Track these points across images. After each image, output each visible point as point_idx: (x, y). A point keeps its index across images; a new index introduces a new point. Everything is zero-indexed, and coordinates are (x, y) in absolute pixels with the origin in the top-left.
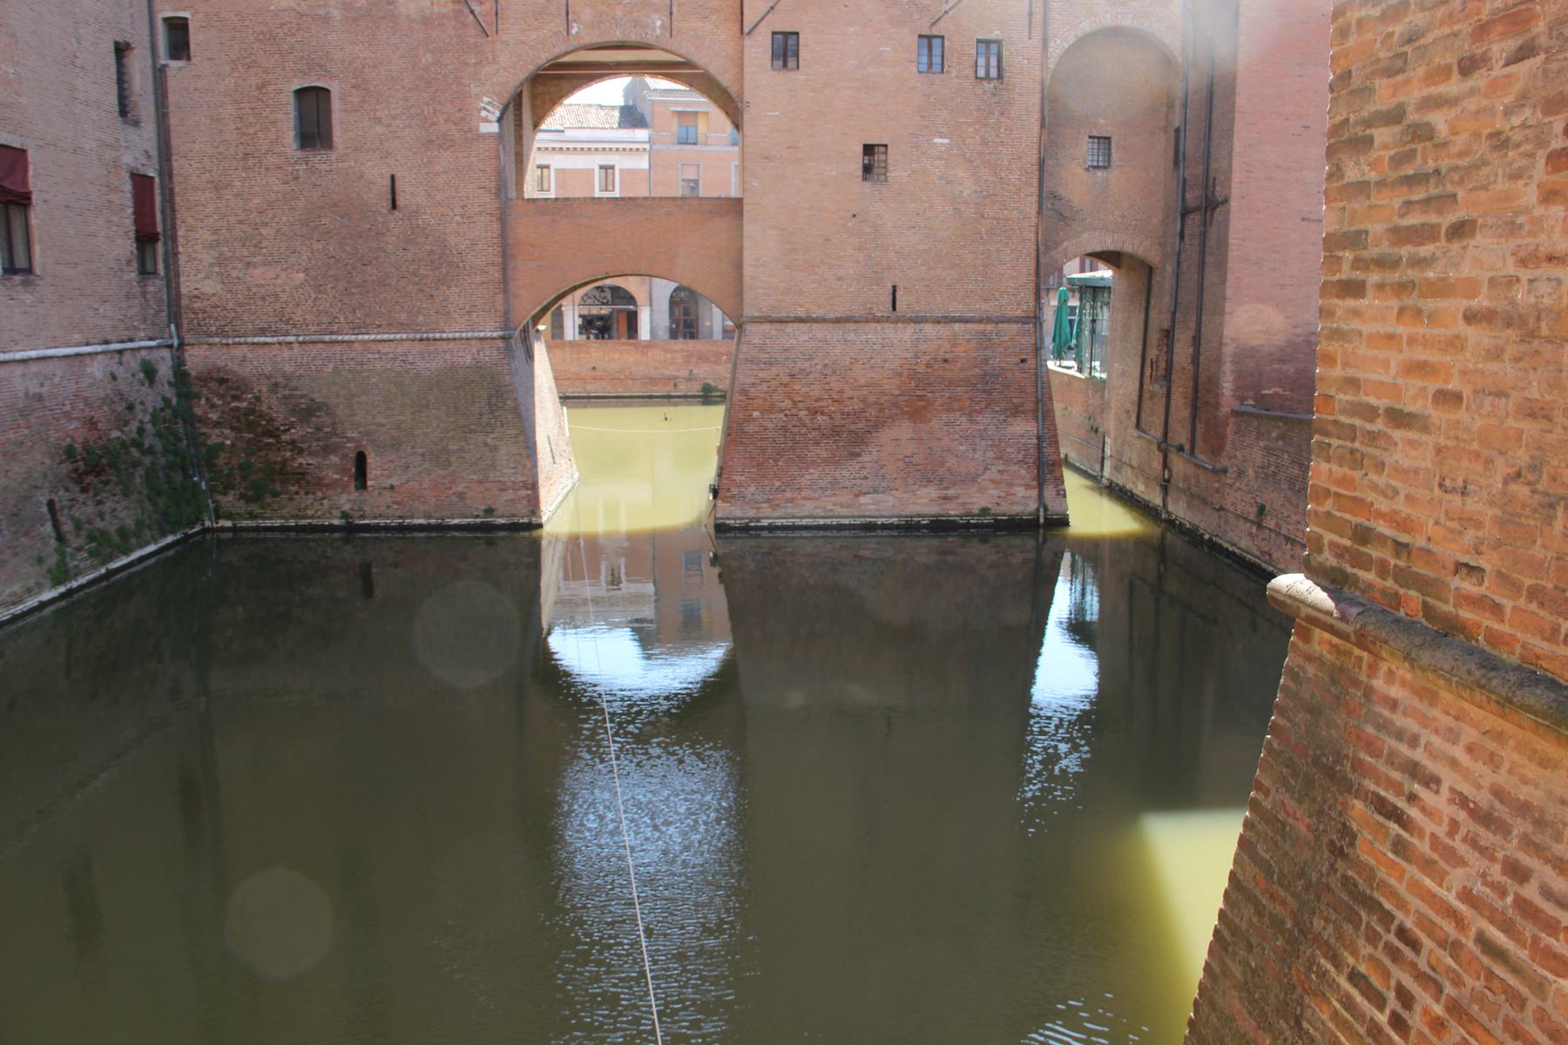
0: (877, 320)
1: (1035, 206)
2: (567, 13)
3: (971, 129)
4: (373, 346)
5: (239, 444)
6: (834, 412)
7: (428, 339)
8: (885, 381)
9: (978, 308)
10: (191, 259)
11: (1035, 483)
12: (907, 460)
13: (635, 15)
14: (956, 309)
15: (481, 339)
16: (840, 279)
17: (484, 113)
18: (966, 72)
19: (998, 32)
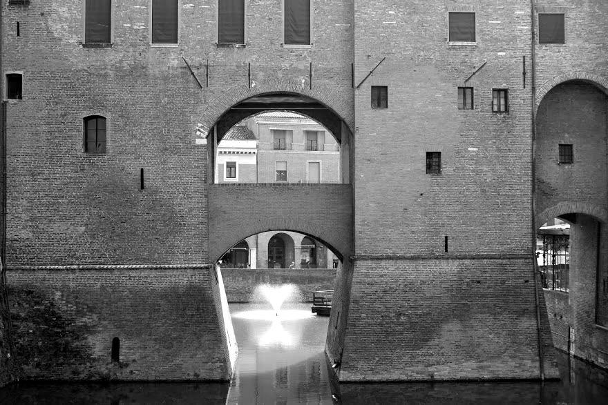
0: (437, 258)
1: (530, 187)
2: (249, 75)
3: (490, 142)
4: (126, 273)
5: (38, 333)
6: (411, 314)
7: (161, 268)
8: (442, 295)
9: (497, 249)
10: (14, 217)
11: (538, 358)
12: (457, 344)
13: (289, 76)
14: (484, 250)
15: (194, 268)
16: (413, 232)
17: (198, 133)
18: (487, 108)
19: (505, 85)
